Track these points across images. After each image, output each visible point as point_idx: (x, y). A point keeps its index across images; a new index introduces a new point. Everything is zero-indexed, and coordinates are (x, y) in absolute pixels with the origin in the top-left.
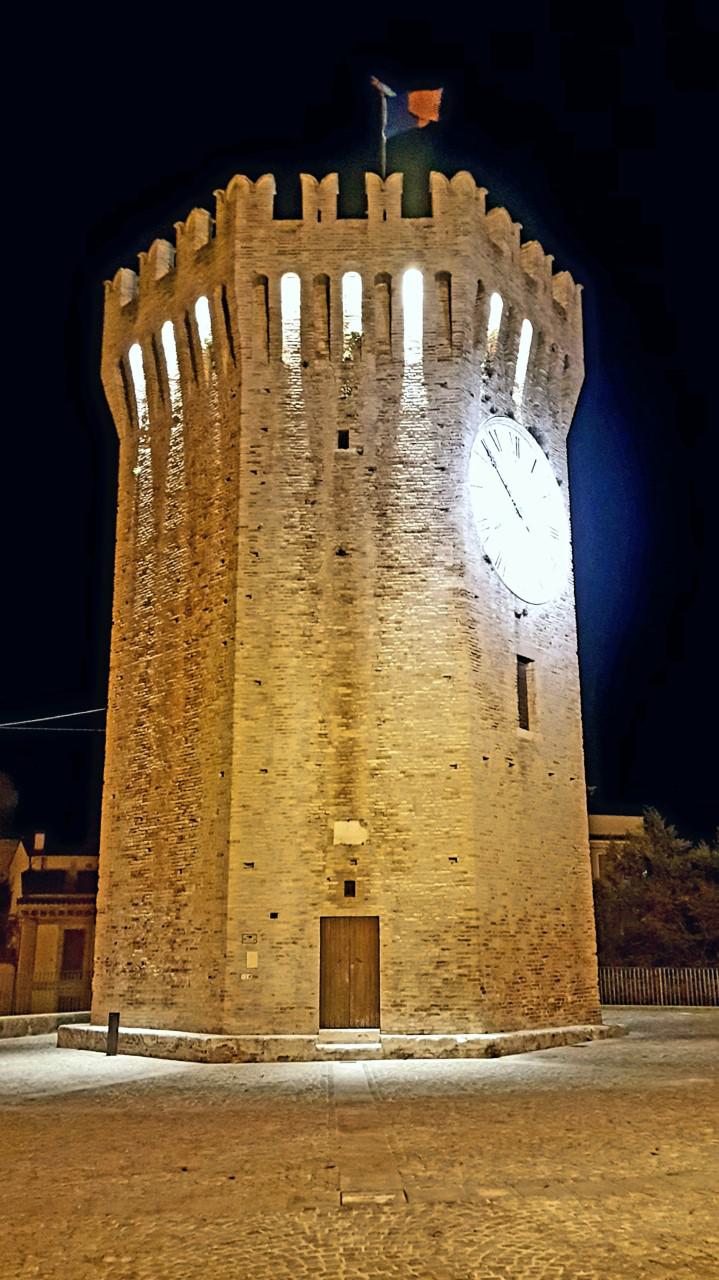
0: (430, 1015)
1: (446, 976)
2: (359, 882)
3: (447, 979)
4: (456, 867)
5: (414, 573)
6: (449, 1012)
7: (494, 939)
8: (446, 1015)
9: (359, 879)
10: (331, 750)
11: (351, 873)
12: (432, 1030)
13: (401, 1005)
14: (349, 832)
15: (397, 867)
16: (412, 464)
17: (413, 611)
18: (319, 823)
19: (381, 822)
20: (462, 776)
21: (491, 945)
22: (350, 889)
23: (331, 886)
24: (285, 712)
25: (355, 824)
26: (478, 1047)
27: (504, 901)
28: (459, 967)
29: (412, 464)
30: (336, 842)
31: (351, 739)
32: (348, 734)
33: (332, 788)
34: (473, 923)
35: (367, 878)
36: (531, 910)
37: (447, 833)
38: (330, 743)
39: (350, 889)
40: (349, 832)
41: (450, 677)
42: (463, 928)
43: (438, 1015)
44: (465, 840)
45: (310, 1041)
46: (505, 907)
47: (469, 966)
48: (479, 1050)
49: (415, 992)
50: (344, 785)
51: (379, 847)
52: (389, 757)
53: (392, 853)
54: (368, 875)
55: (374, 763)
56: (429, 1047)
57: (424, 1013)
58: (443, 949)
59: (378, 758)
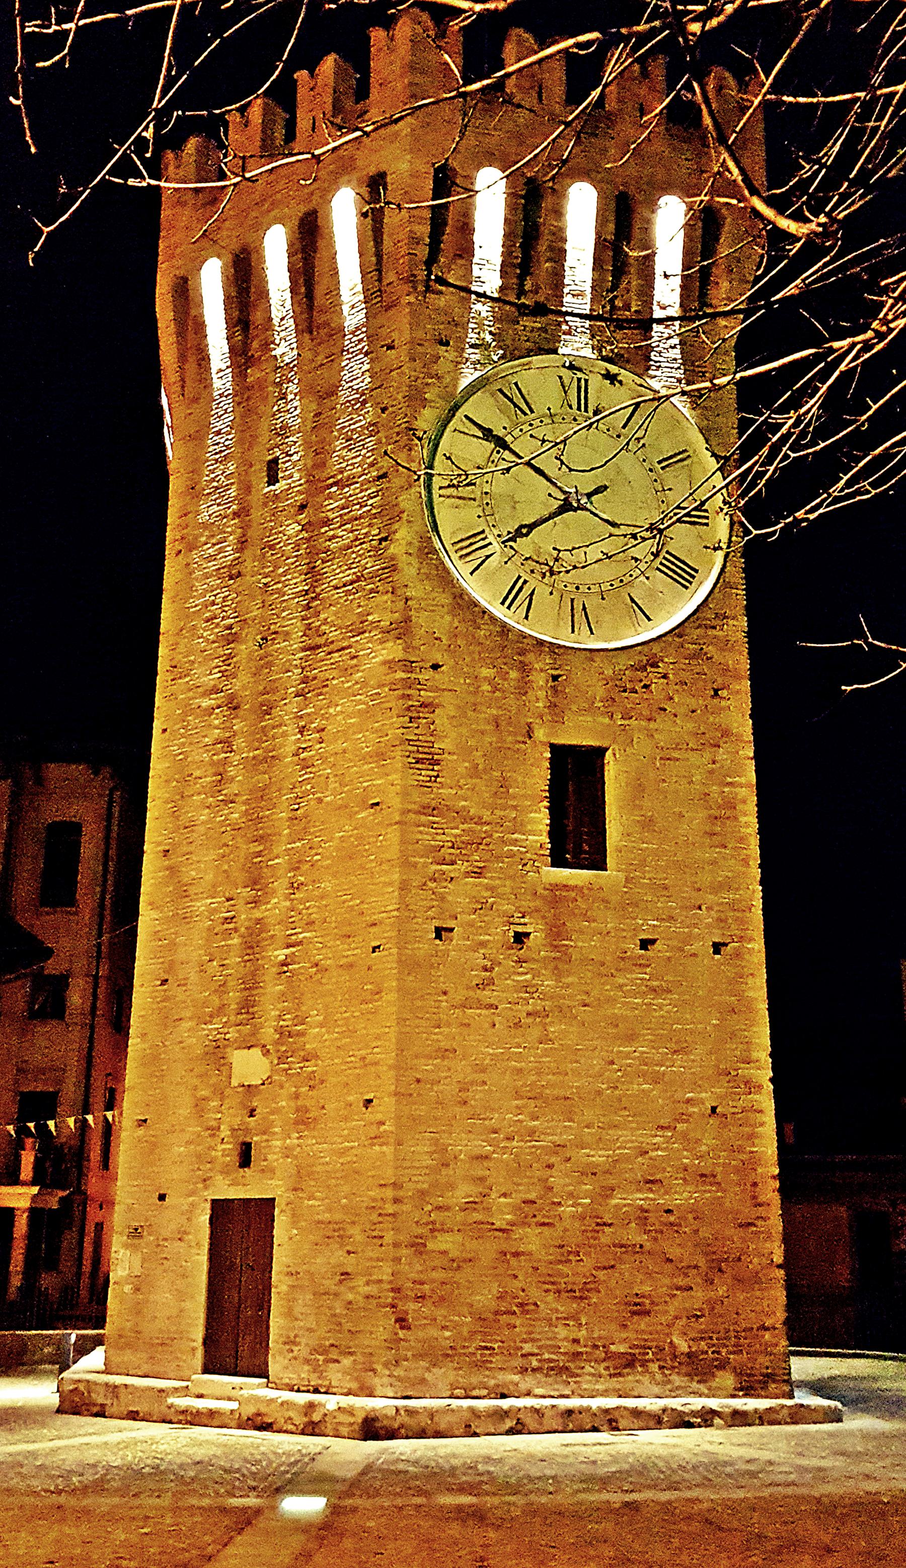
0: (327, 1361)
1: (350, 1297)
2: (256, 1143)
3: (350, 1303)
4: (371, 1115)
5: (343, 649)
6: (352, 1358)
7: (440, 1237)
8: (347, 1362)
9: (255, 1139)
10: (236, 941)
11: (247, 1131)
12: (328, 1388)
13: (294, 1343)
14: (249, 1066)
15: (303, 1121)
16: (350, 482)
17: (339, 708)
18: (217, 1054)
20: (387, 962)
21: (430, 1246)
24: (192, 890)
25: (256, 1052)
26: (352, 1420)
28: (367, 1283)
29: (350, 482)
30: (235, 1082)
31: (259, 921)
32: (258, 914)
33: (234, 997)
34: (390, 1208)
35: (265, 1137)
37: (363, 1059)
38: (236, 930)
40: (249, 1066)
41: (377, 804)
42: (374, 1217)
43: (337, 1361)
44: (385, 1068)
45: (161, 1391)
46: (482, 1179)
47: (380, 1281)
48: (351, 1424)
49: (311, 1323)
50: (246, 993)
51: (282, 1087)
52: (300, 943)
53: (297, 1096)
54: (264, 1133)
55: (281, 954)
56: (291, 1414)
57: (321, 1358)
58: (349, 1252)
59: (288, 947)
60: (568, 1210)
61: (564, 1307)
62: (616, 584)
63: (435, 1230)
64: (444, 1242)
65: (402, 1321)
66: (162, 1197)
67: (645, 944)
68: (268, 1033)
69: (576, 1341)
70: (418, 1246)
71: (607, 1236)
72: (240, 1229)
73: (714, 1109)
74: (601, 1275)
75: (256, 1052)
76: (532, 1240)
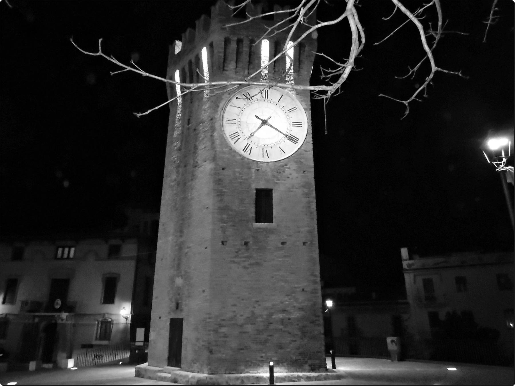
4: (205, 294)
19: (186, 277)
22: (178, 306)
23: (173, 305)
25: (180, 278)
27: (234, 309)
30: (176, 286)
34: (208, 320)
36: (257, 311)
39: (178, 306)
40: (179, 281)
46: (234, 311)
60: (259, 319)
61: (260, 347)
62: (276, 144)
63: (221, 326)
64: (223, 330)
65: (211, 352)
66: (160, 318)
67: (283, 243)
68: (183, 273)
69: (262, 357)
70: (216, 331)
71: (272, 327)
72: (176, 327)
73: (303, 290)
74: (269, 338)
75: (180, 278)
76: (249, 328)
